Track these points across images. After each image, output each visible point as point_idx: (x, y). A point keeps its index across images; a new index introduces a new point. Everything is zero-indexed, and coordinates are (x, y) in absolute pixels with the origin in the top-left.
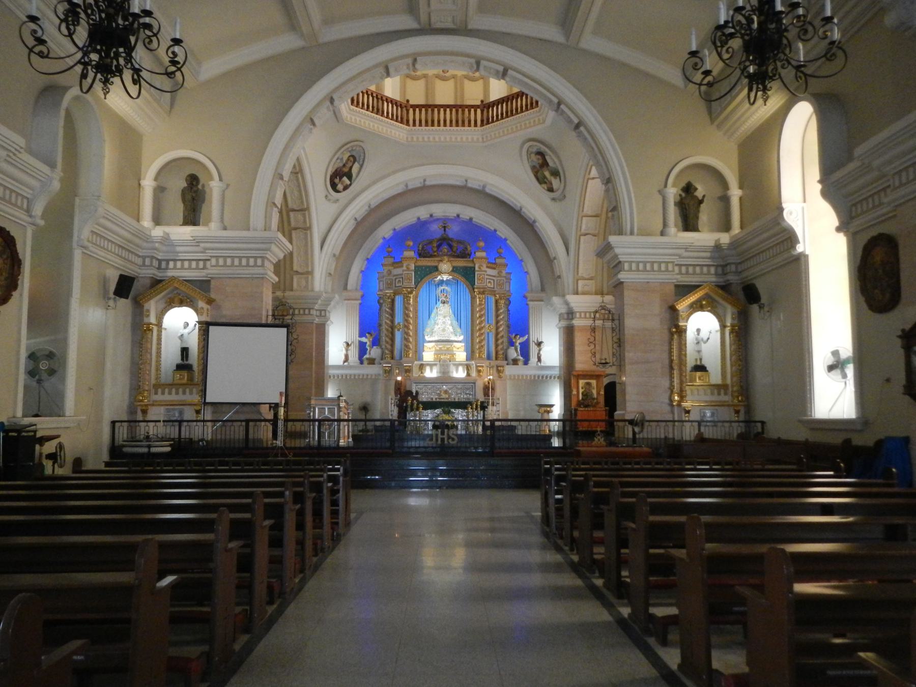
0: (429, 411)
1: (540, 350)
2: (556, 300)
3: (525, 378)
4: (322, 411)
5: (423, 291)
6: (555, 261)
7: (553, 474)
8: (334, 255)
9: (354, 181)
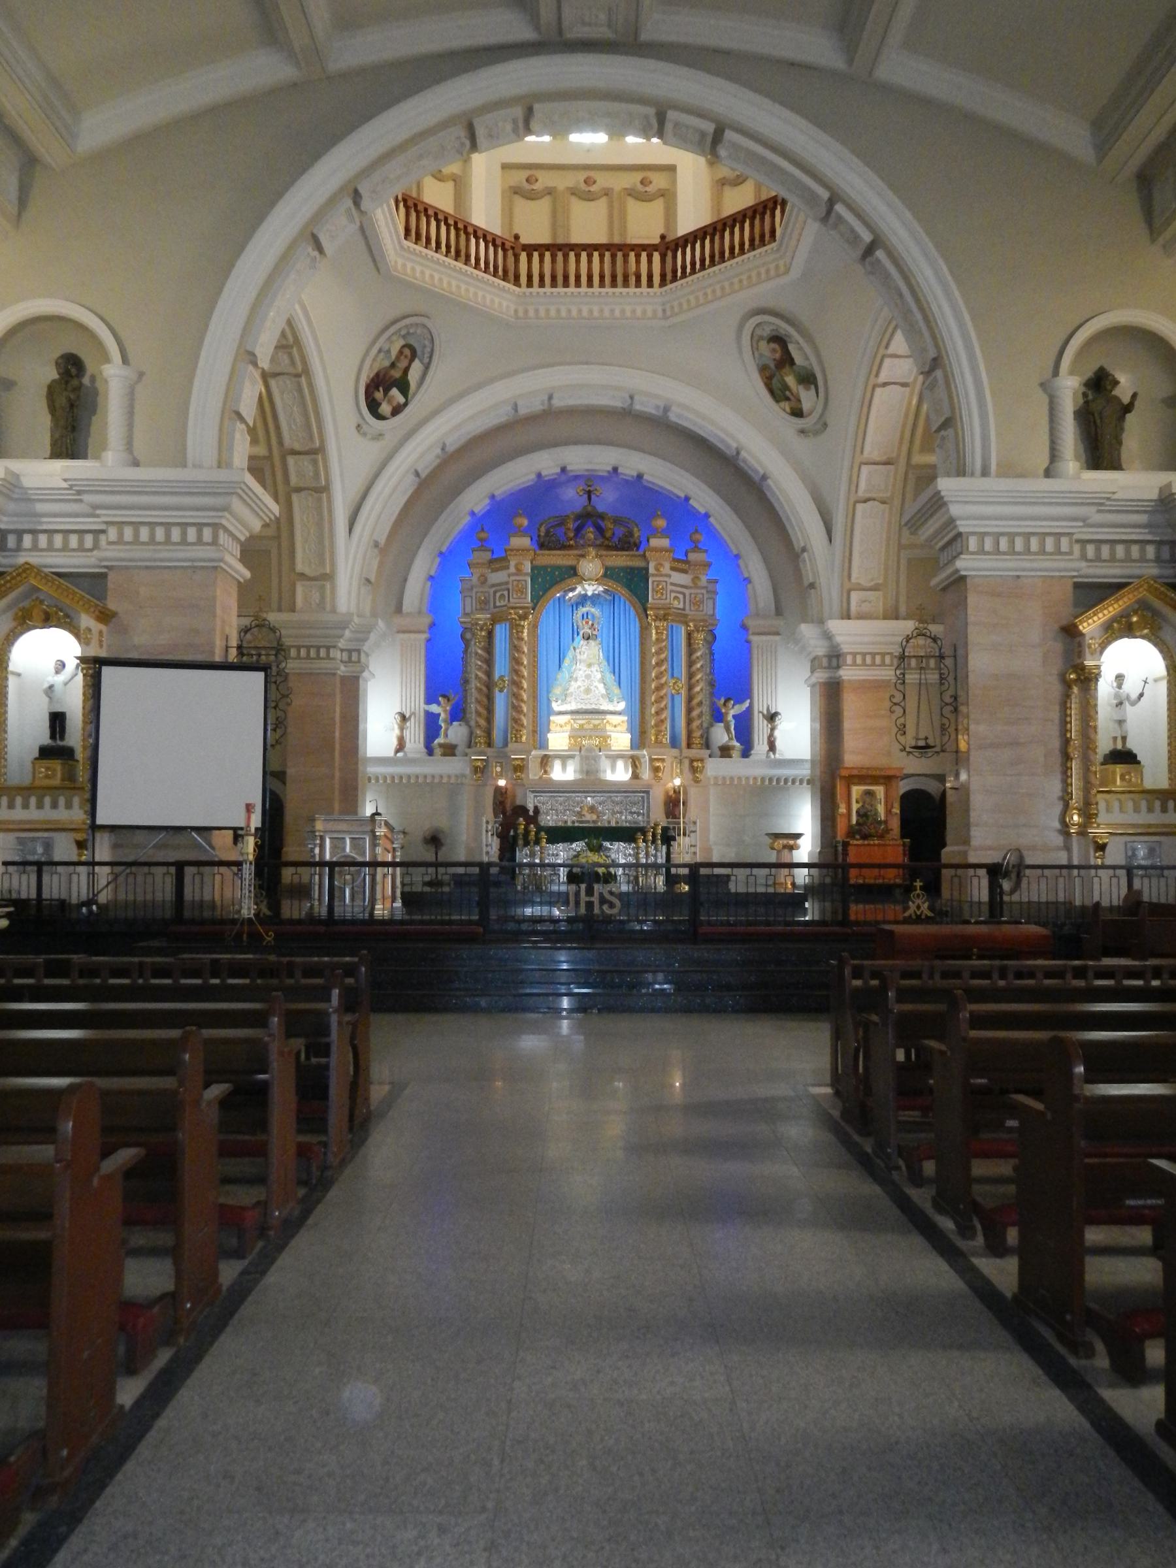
0: (560, 846)
1: (773, 729)
2: (807, 631)
3: (744, 782)
4: (338, 843)
5: (548, 616)
6: (805, 554)
7: (891, 1011)
8: (376, 544)
9: (415, 394)
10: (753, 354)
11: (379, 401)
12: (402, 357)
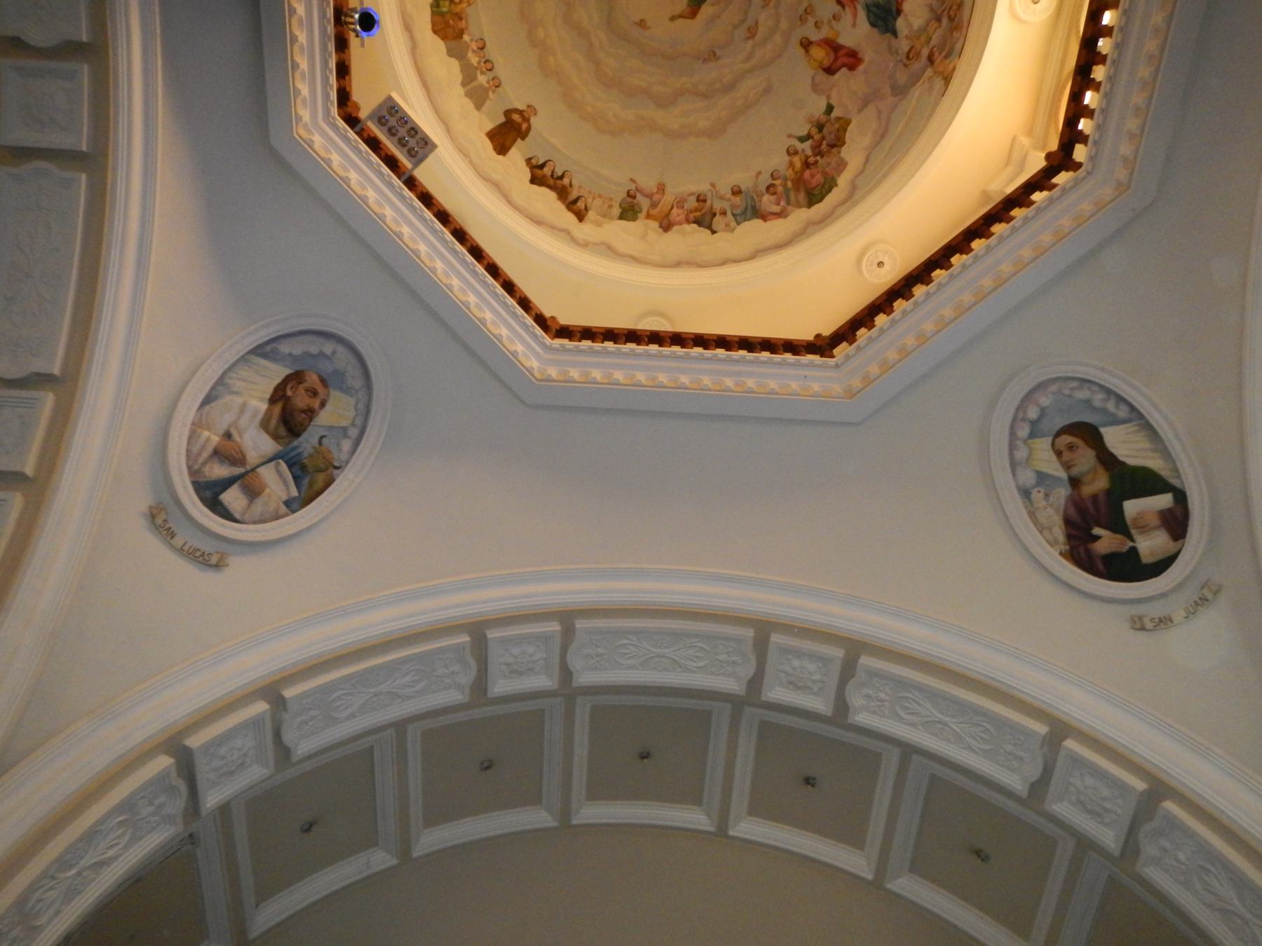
9: (1175, 470)
11: (1125, 549)
12: (1067, 456)
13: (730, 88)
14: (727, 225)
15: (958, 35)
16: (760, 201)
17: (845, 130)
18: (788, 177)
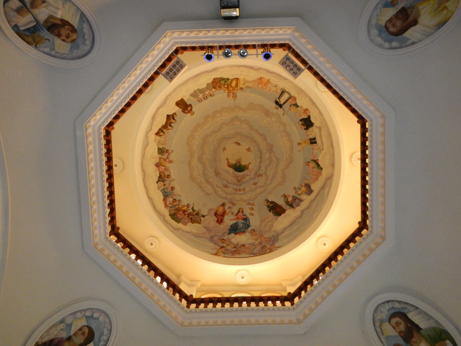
10: (380, 339)
12: (81, 332)
13: (207, 181)
14: (160, 187)
15: (231, 255)
16: (170, 197)
17: (197, 223)
18: (179, 206)
